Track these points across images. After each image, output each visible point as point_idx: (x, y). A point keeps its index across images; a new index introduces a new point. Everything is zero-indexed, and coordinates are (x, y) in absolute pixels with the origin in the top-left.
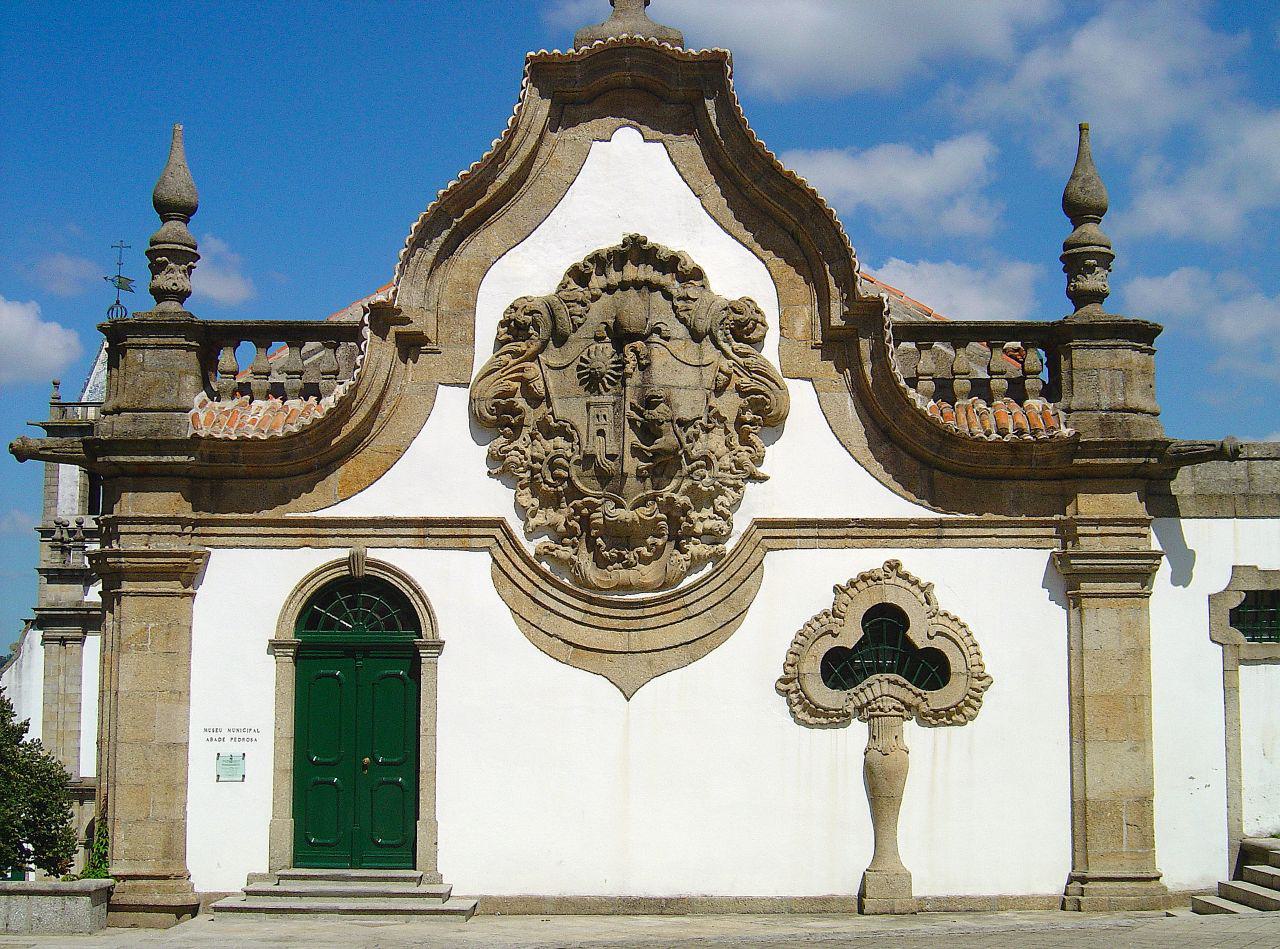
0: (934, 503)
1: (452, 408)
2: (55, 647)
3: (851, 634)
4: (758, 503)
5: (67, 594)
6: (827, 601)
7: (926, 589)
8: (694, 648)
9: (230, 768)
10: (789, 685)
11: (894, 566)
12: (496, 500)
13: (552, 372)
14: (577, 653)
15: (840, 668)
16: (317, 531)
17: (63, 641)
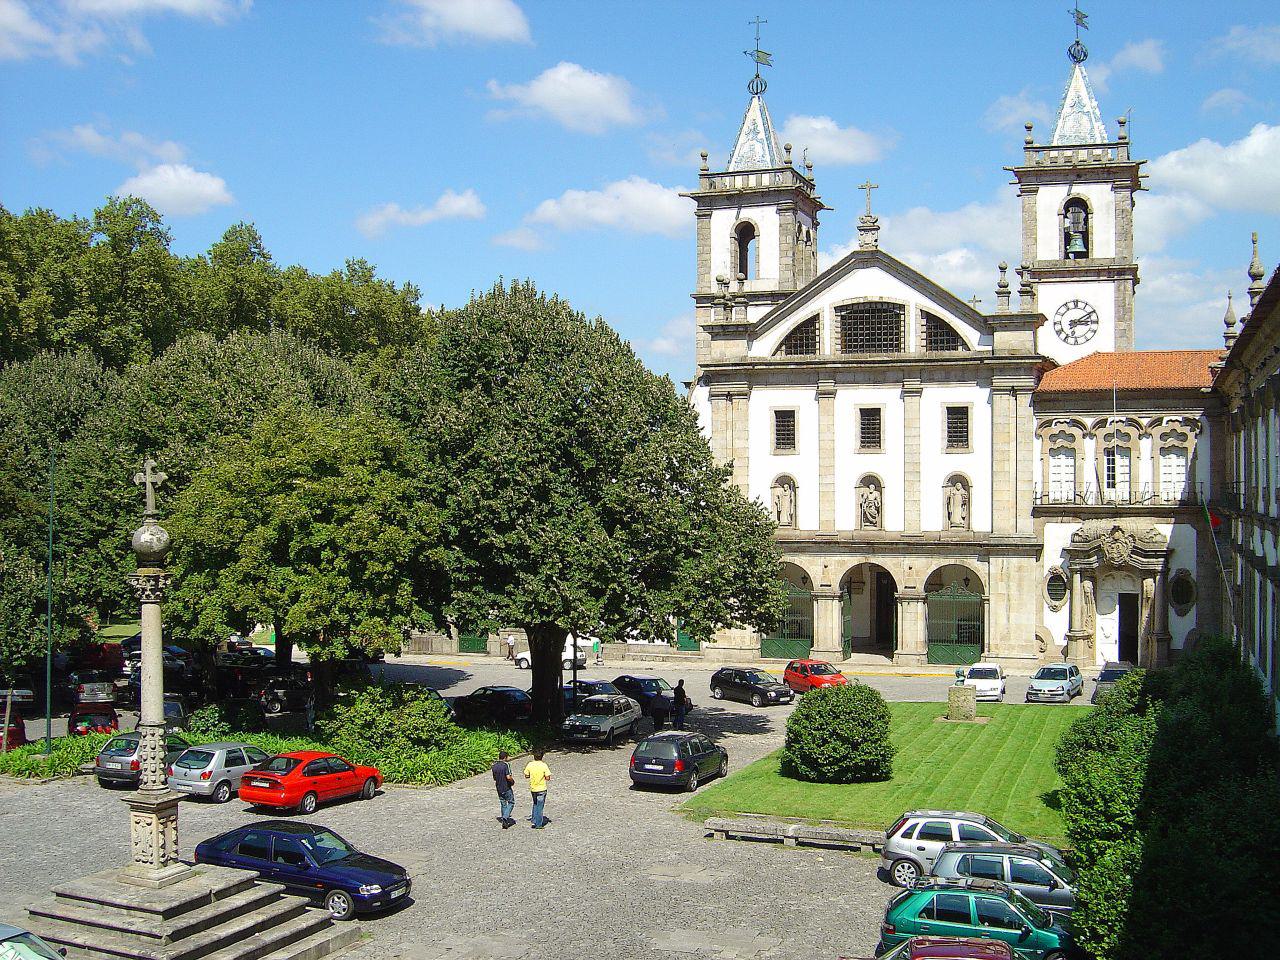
2: (722, 403)
5: (732, 350)
17: (729, 396)
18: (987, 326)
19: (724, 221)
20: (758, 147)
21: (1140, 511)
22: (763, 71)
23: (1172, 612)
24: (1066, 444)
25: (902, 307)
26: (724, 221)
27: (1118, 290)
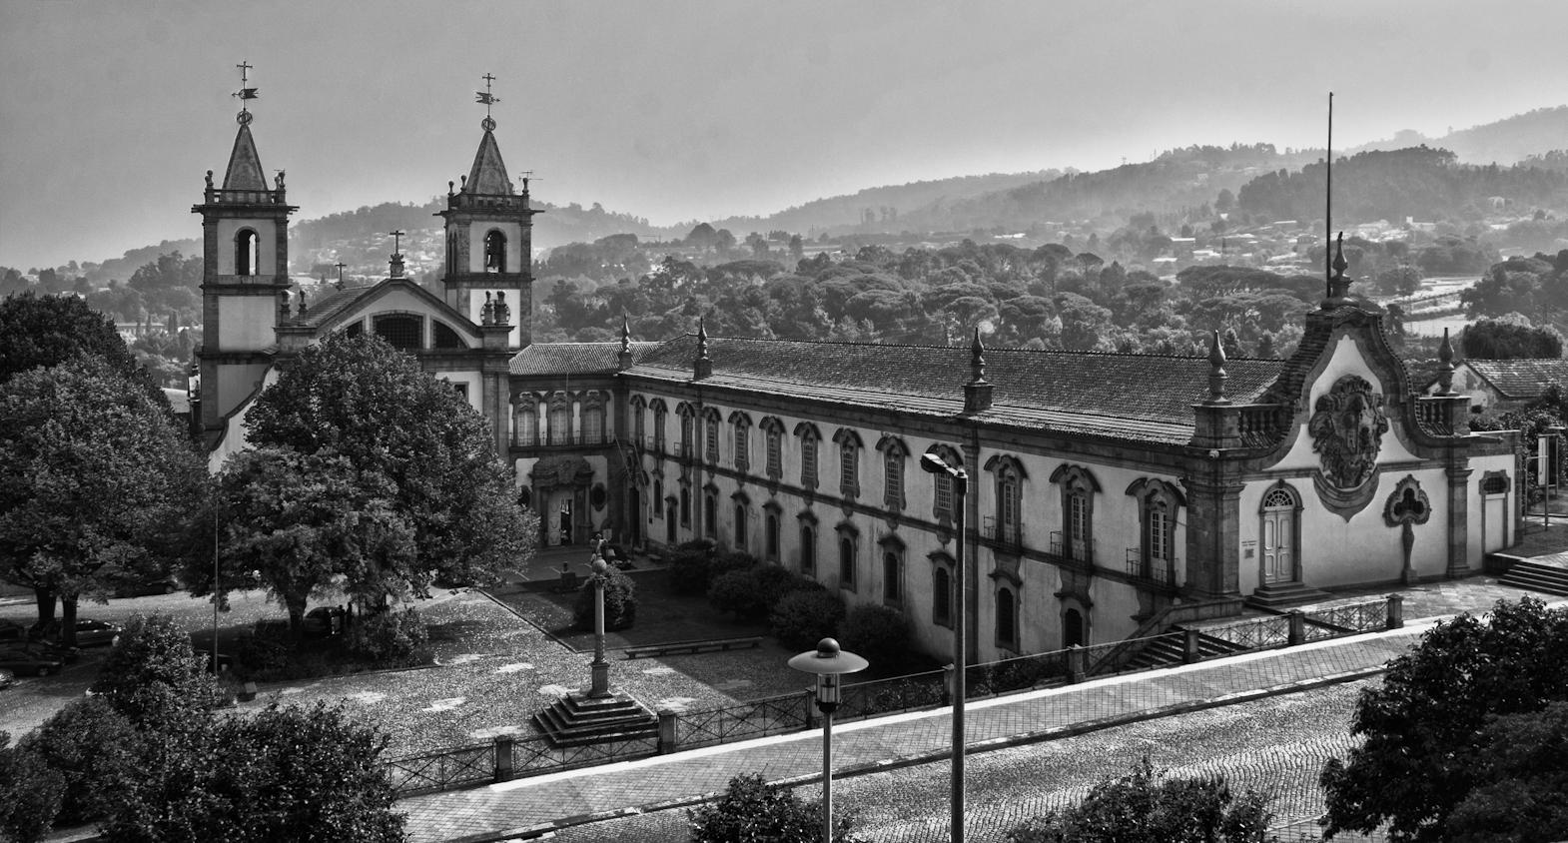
0: (1418, 455)
1: (1304, 428)
3: (1401, 498)
4: (1381, 458)
6: (1393, 489)
7: (1418, 483)
8: (1363, 506)
9: (1249, 554)
10: (1386, 515)
11: (1410, 476)
12: (1314, 460)
13: (1335, 420)
14: (1335, 509)
15: (1399, 510)
16: (1270, 475)
18: (477, 331)
19: (228, 230)
20: (251, 170)
21: (1168, 549)
22: (251, 106)
23: (593, 508)
24: (530, 405)
25: (421, 317)
26: (228, 230)
27: (522, 295)
